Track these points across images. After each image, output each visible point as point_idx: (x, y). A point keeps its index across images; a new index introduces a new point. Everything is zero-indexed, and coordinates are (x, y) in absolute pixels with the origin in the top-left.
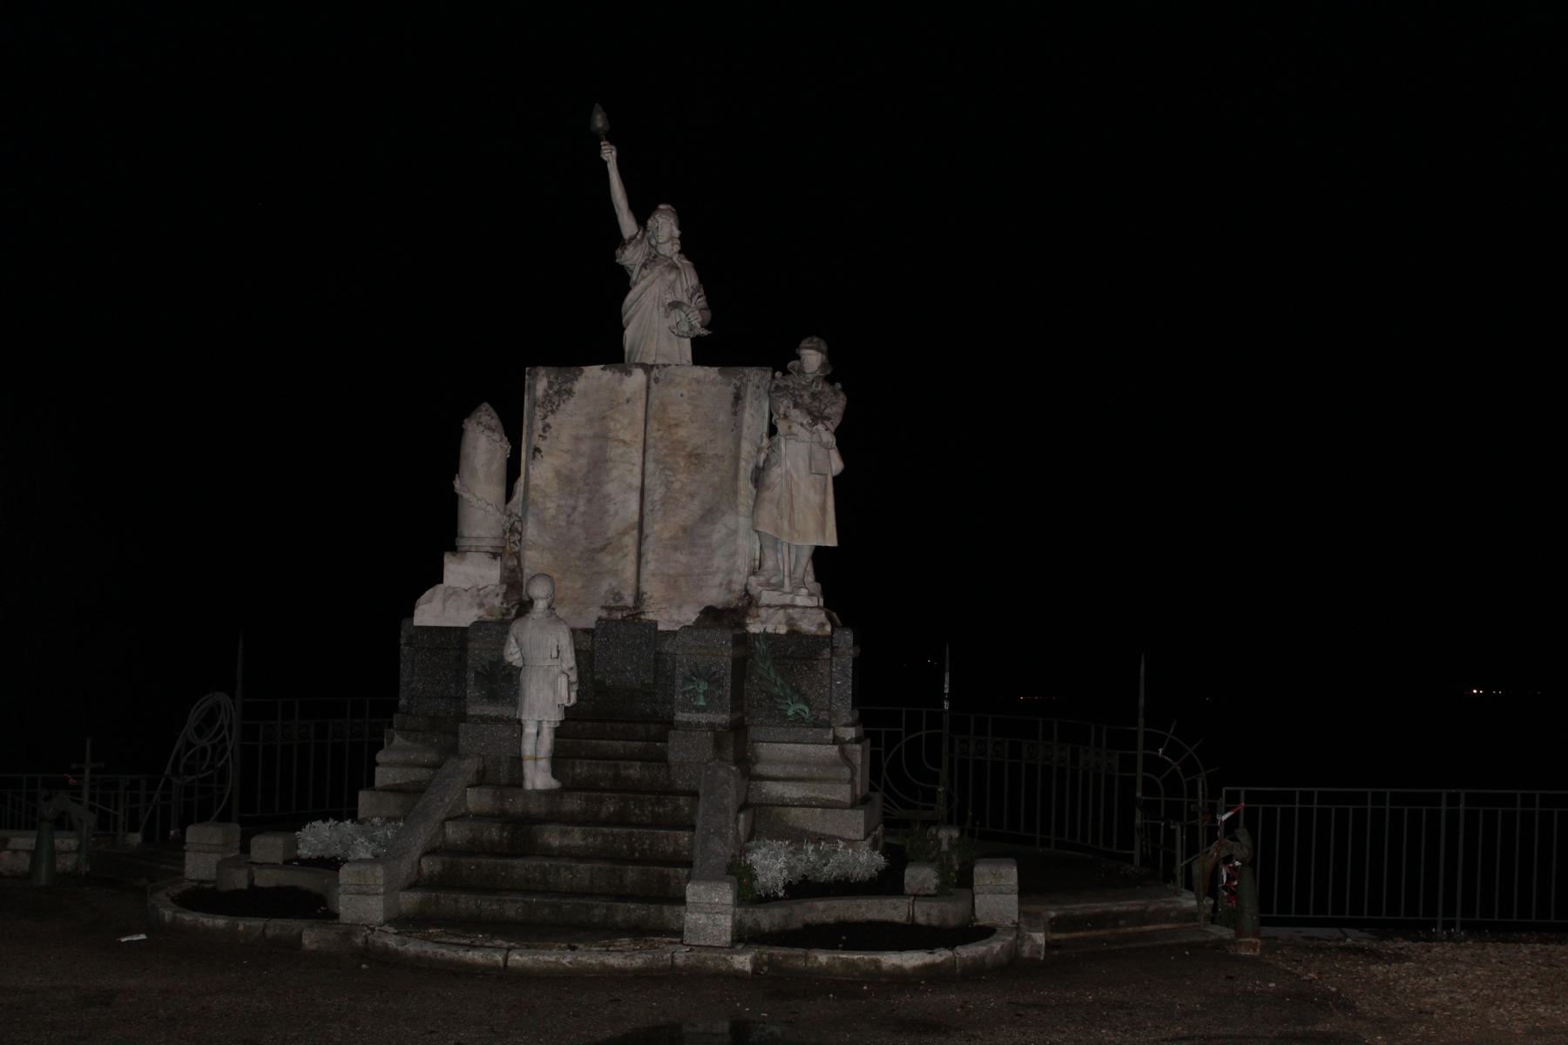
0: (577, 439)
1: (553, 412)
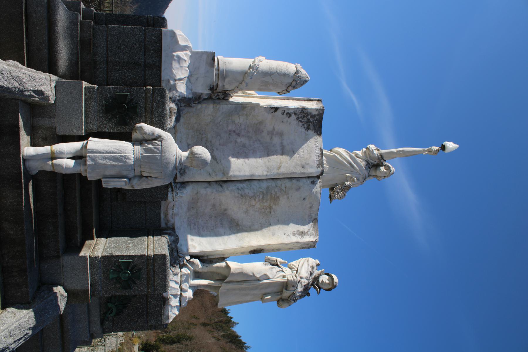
0: (281, 134)
1: (298, 118)
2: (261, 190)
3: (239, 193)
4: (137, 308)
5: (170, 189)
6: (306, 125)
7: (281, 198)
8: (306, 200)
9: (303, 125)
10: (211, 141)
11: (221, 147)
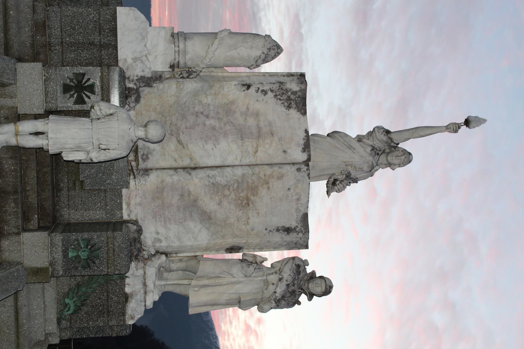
0: (257, 115)
1: (276, 96)
2: (236, 178)
3: (209, 181)
4: (96, 306)
5: (132, 177)
6: (286, 104)
7: (260, 188)
8: (292, 191)
9: (283, 103)
10: (176, 125)
11: (188, 130)
